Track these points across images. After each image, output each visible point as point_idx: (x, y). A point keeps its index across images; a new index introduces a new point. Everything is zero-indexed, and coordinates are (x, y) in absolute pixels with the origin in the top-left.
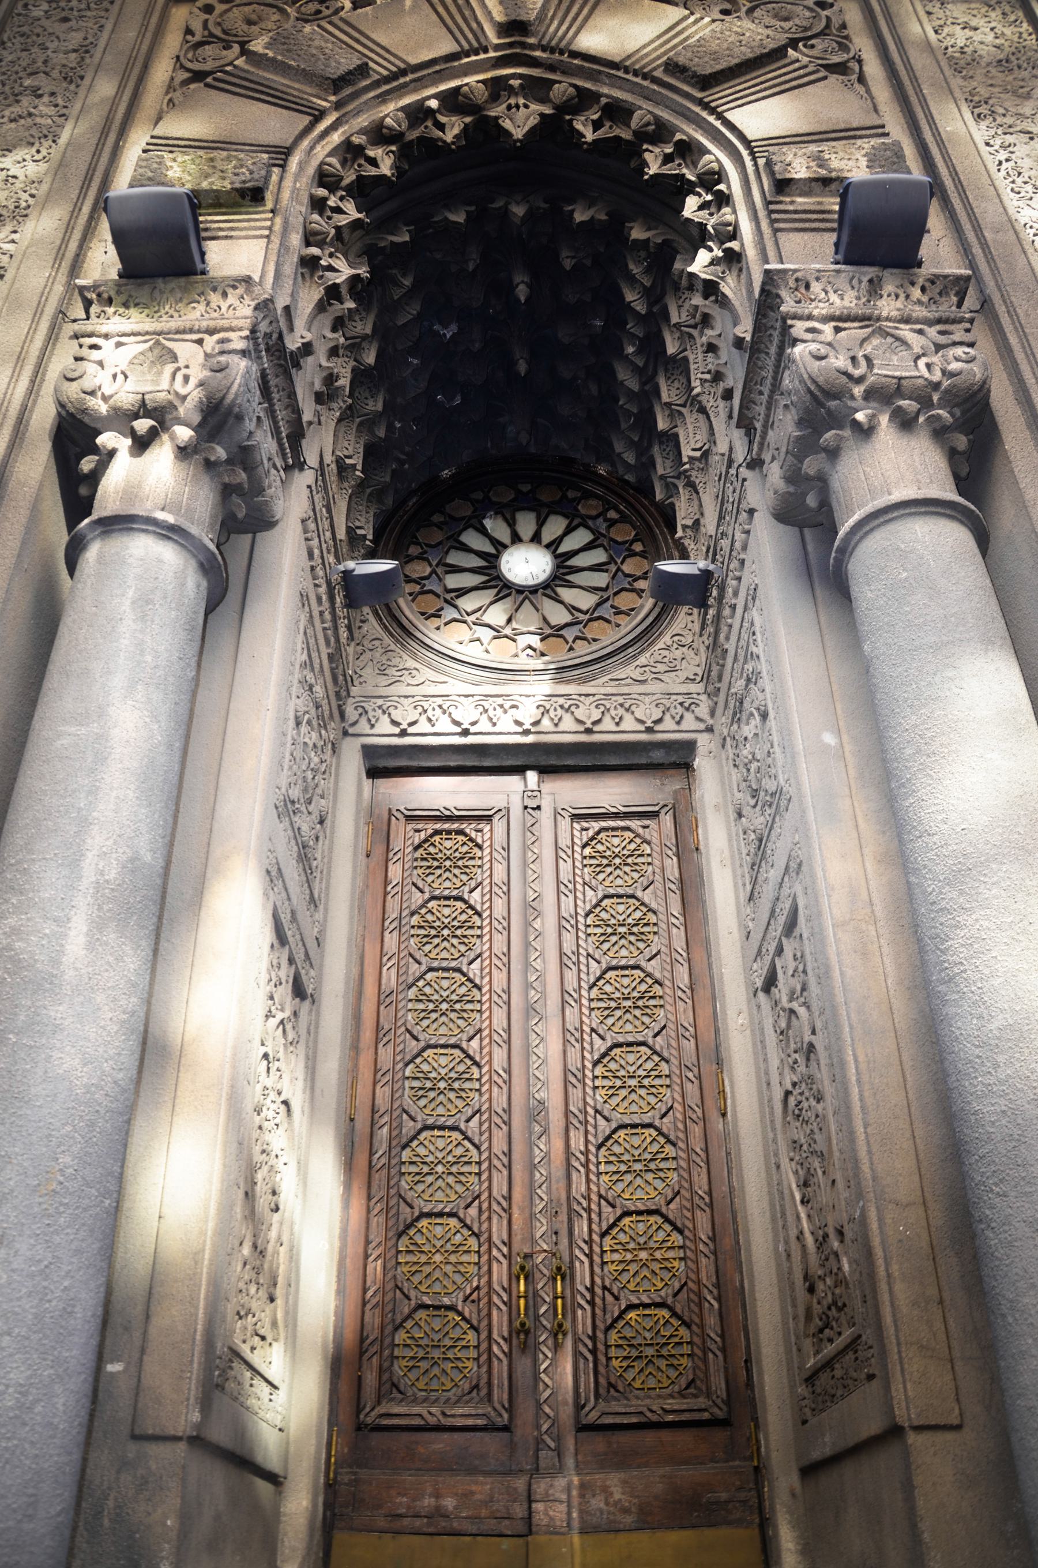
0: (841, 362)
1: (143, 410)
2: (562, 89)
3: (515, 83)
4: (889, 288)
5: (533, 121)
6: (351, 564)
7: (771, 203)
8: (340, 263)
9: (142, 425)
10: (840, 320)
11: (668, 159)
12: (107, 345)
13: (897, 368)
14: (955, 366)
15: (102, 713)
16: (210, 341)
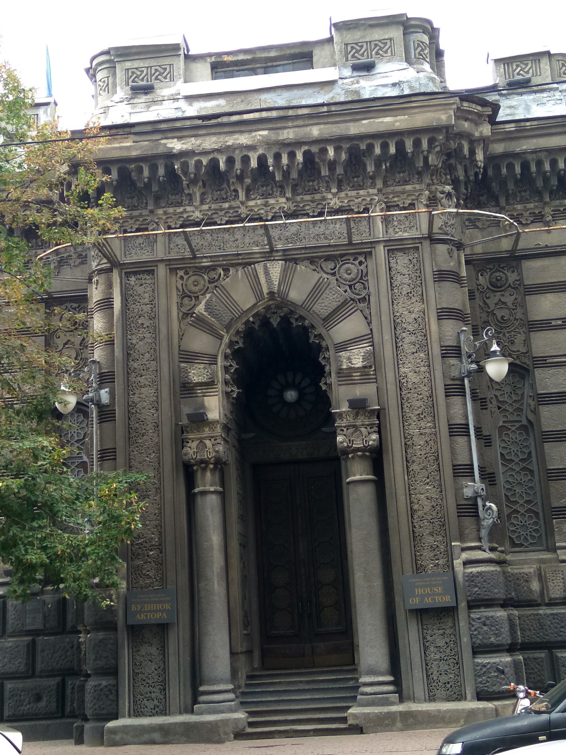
0: (345, 444)
1: (202, 461)
2: (285, 310)
3: (273, 306)
4: (361, 413)
5: (279, 319)
6: (244, 436)
7: (339, 373)
8: (235, 389)
9: (203, 465)
10: (348, 427)
11: (315, 336)
12: (190, 441)
13: (358, 444)
14: (371, 443)
15: (210, 539)
16: (212, 440)
